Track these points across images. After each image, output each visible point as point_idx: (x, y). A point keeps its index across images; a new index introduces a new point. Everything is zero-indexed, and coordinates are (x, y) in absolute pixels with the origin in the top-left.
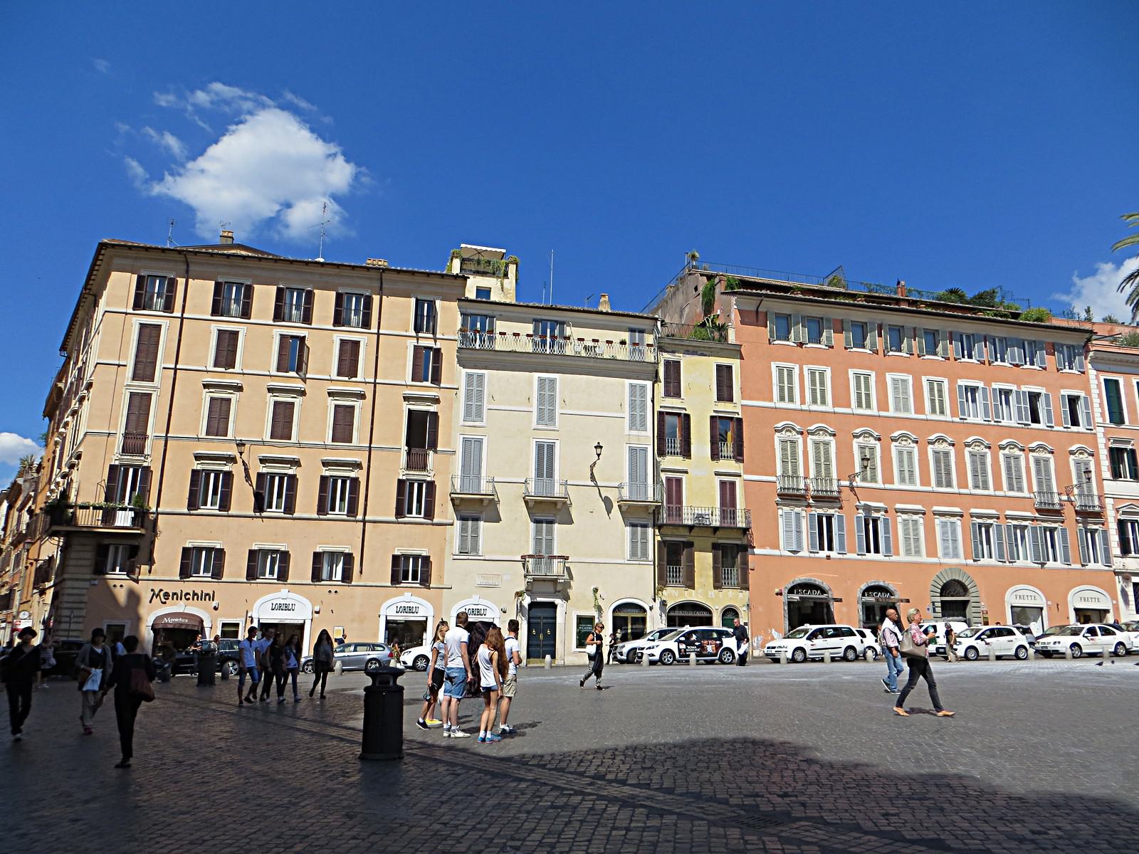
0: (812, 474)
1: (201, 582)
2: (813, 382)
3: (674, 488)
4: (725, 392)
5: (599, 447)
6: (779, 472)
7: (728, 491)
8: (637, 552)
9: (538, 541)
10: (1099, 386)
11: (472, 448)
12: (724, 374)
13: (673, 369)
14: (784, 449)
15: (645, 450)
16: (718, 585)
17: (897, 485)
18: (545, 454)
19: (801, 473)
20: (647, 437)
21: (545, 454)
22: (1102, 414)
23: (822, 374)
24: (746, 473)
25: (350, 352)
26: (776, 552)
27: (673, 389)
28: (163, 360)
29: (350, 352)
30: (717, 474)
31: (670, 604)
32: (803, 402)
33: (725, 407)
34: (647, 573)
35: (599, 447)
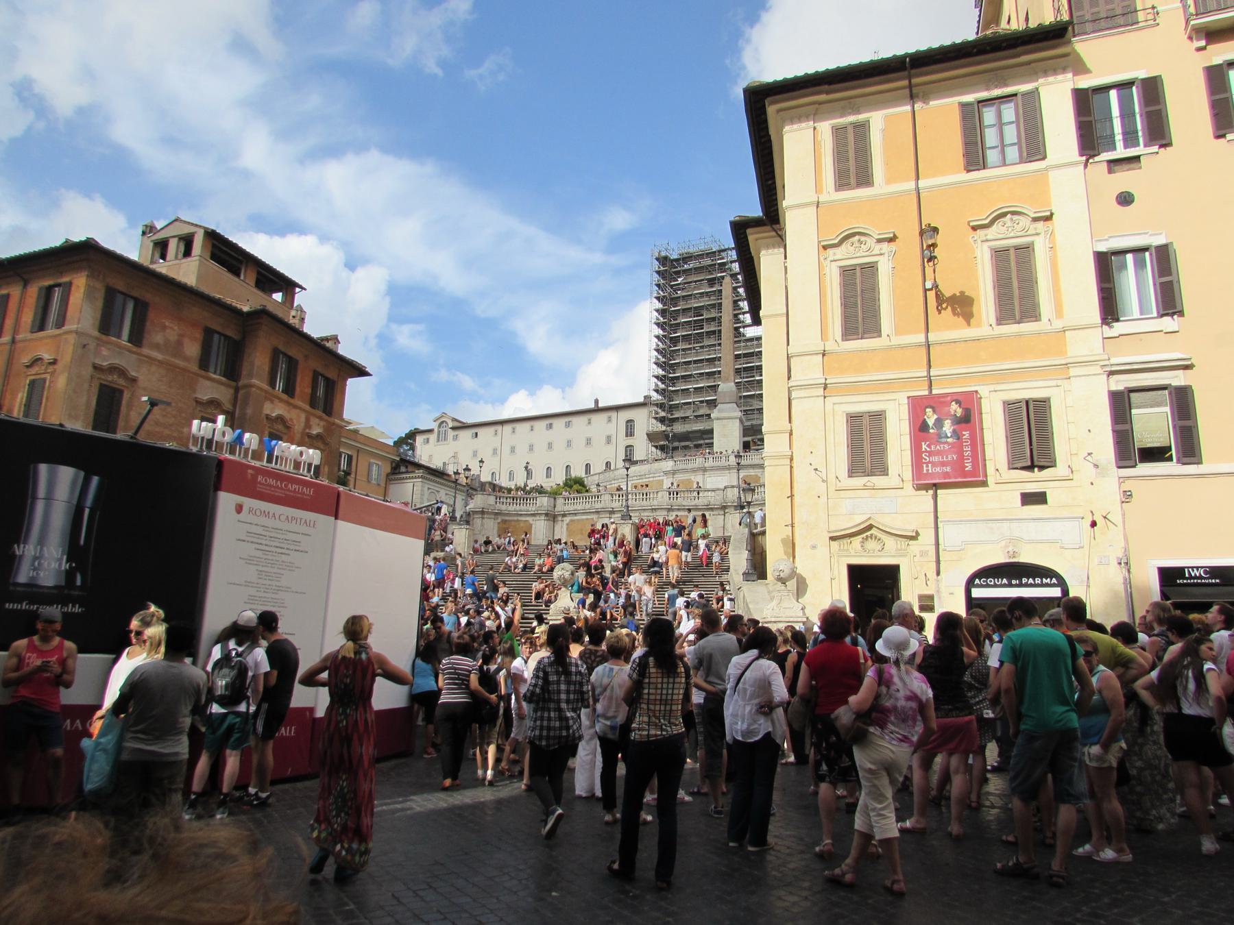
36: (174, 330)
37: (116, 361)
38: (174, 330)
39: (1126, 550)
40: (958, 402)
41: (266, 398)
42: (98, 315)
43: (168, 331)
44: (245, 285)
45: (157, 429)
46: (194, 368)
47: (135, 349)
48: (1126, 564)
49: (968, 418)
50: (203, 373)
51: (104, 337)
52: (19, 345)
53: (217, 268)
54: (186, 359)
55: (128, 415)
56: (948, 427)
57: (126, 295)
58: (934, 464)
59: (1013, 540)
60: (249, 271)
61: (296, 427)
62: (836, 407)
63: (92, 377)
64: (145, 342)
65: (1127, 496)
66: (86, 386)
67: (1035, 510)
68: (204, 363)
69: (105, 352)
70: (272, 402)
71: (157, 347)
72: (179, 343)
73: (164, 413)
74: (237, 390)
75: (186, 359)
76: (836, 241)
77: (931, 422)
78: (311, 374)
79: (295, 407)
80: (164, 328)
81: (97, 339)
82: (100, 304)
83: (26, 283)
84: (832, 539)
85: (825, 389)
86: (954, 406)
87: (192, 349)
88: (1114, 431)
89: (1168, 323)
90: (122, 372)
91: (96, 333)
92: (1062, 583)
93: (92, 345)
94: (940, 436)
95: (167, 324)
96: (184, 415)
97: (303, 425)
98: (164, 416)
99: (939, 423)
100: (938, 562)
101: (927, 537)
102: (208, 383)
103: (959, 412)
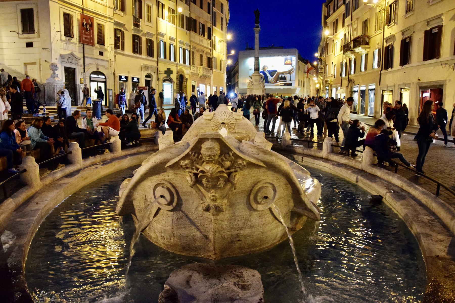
39: (114, 70)
40: (90, 20)
48: (114, 74)
49: (92, 26)
56: (88, 27)
58: (86, 38)
59: (98, 65)
62: (61, 8)
65: (115, 57)
67: (101, 57)
77: (85, 24)
86: (89, 21)
89: (121, 13)
92: (105, 78)
94: (87, 29)
99: (86, 24)
100: (84, 68)
101: (81, 61)
103: (90, 23)
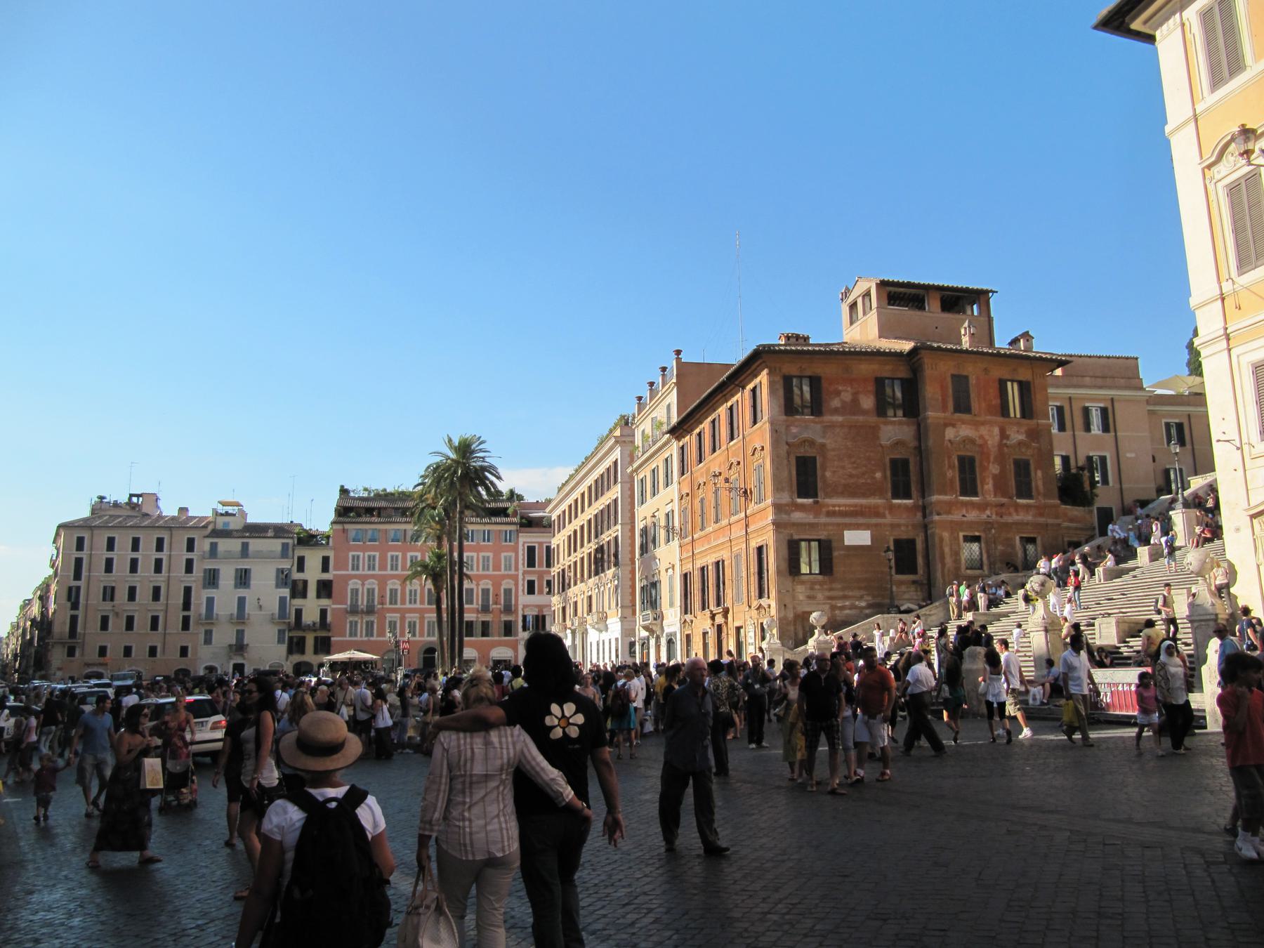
0: (365, 603)
1: (102, 660)
2: (369, 560)
3: (299, 613)
4: (325, 568)
5: (259, 599)
6: (349, 603)
7: (323, 613)
8: (280, 641)
9: (237, 638)
10: (523, 550)
11: (210, 601)
12: (326, 561)
13: (301, 561)
14: (352, 593)
15: (286, 597)
16: (316, 652)
17: (408, 606)
18: (242, 601)
19: (360, 603)
20: (286, 592)
21: (242, 601)
22: (523, 564)
23: (374, 557)
24: (333, 604)
25: (158, 565)
26: (345, 639)
27: (301, 568)
28: (84, 573)
29: (158, 565)
30: (319, 606)
31: (295, 662)
32: (363, 570)
33: (326, 576)
34: (284, 648)
35: (259, 599)
36: (848, 391)
37: (805, 435)
38: (848, 391)
41: (946, 425)
42: (782, 401)
43: (842, 394)
44: (931, 315)
45: (852, 481)
46: (873, 419)
47: (817, 419)
50: (882, 419)
51: (790, 418)
52: (747, 439)
53: (897, 312)
54: (864, 412)
55: (823, 476)
57: (800, 378)
60: (931, 301)
61: (989, 442)
63: (788, 453)
64: (824, 409)
66: (785, 462)
68: (881, 408)
69: (794, 430)
70: (954, 426)
71: (836, 411)
72: (855, 401)
73: (855, 465)
74: (919, 425)
75: (864, 412)
76: (1213, 159)
78: (997, 385)
79: (983, 423)
80: (838, 393)
81: (786, 421)
82: (781, 392)
83: (744, 388)
84: (1253, 517)
85: (1228, 339)
87: (868, 402)
88: (1206, 406)
90: (812, 443)
91: (784, 417)
93: (783, 429)
95: (840, 388)
96: (873, 462)
97: (997, 438)
98: (856, 468)
102: (890, 428)
